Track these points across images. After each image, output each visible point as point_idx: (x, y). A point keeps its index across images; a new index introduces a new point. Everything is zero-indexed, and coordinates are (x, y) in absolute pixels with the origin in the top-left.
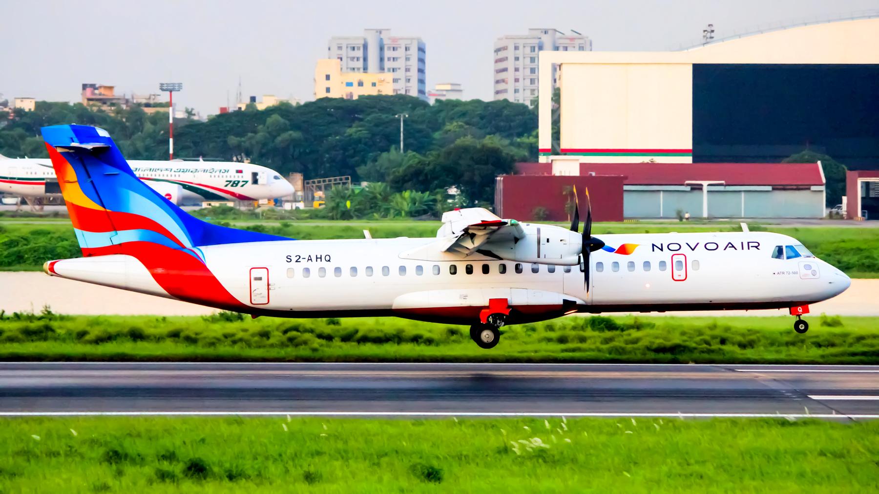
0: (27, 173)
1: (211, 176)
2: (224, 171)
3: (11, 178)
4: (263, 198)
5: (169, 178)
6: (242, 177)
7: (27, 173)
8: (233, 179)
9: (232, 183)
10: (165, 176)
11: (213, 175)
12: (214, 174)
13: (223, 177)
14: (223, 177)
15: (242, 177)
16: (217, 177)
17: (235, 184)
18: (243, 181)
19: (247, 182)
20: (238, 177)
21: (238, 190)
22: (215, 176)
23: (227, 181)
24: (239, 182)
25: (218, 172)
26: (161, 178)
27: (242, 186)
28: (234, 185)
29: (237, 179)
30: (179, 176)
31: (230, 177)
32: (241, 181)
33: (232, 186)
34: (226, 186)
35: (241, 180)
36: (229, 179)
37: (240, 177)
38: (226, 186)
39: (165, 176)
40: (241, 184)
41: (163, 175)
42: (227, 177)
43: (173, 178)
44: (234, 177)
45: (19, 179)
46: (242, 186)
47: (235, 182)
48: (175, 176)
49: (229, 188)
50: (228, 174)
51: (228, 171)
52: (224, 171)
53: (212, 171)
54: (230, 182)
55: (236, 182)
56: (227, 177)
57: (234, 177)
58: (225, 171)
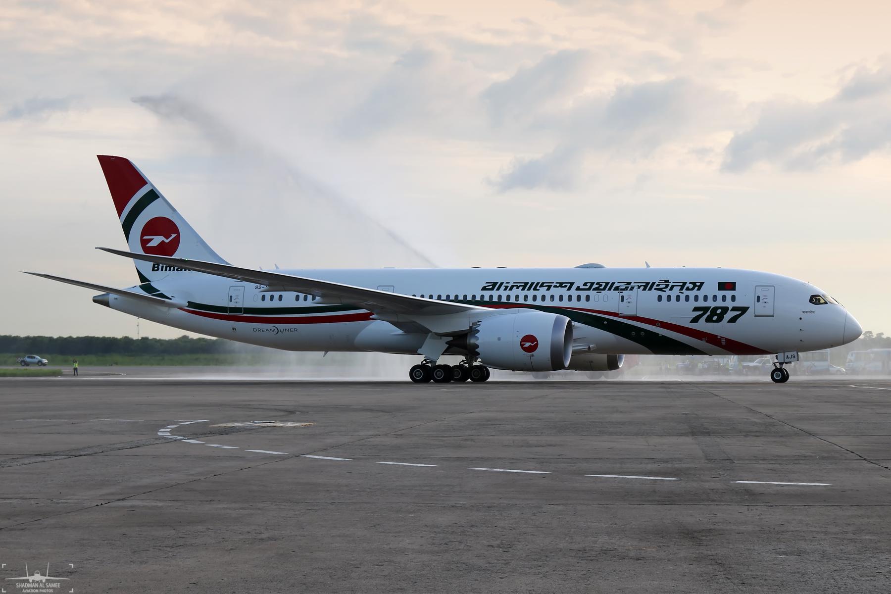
0: (263, 298)
1: (660, 298)
2: (691, 286)
5: (565, 304)
6: (733, 298)
8: (710, 304)
9: (708, 313)
10: (557, 298)
11: (664, 295)
12: (668, 292)
13: (687, 298)
14: (687, 298)
16: (673, 298)
17: (716, 315)
18: (734, 309)
19: (744, 310)
20: (724, 298)
22: (669, 298)
23: (696, 309)
24: (725, 310)
25: (676, 290)
26: (548, 303)
27: (733, 320)
28: (715, 318)
29: (719, 303)
31: (706, 298)
32: (730, 309)
33: (709, 320)
35: (729, 304)
36: (701, 303)
37: (729, 298)
38: (695, 320)
39: (557, 298)
40: (730, 315)
41: (552, 297)
42: (696, 298)
43: (574, 304)
44: (715, 298)
46: (733, 320)
47: (716, 308)
49: (702, 326)
50: (701, 294)
51: (702, 284)
52: (691, 286)
53: (661, 286)
54: (705, 309)
55: (719, 311)
56: (696, 298)
57: (715, 298)
58: (694, 284)
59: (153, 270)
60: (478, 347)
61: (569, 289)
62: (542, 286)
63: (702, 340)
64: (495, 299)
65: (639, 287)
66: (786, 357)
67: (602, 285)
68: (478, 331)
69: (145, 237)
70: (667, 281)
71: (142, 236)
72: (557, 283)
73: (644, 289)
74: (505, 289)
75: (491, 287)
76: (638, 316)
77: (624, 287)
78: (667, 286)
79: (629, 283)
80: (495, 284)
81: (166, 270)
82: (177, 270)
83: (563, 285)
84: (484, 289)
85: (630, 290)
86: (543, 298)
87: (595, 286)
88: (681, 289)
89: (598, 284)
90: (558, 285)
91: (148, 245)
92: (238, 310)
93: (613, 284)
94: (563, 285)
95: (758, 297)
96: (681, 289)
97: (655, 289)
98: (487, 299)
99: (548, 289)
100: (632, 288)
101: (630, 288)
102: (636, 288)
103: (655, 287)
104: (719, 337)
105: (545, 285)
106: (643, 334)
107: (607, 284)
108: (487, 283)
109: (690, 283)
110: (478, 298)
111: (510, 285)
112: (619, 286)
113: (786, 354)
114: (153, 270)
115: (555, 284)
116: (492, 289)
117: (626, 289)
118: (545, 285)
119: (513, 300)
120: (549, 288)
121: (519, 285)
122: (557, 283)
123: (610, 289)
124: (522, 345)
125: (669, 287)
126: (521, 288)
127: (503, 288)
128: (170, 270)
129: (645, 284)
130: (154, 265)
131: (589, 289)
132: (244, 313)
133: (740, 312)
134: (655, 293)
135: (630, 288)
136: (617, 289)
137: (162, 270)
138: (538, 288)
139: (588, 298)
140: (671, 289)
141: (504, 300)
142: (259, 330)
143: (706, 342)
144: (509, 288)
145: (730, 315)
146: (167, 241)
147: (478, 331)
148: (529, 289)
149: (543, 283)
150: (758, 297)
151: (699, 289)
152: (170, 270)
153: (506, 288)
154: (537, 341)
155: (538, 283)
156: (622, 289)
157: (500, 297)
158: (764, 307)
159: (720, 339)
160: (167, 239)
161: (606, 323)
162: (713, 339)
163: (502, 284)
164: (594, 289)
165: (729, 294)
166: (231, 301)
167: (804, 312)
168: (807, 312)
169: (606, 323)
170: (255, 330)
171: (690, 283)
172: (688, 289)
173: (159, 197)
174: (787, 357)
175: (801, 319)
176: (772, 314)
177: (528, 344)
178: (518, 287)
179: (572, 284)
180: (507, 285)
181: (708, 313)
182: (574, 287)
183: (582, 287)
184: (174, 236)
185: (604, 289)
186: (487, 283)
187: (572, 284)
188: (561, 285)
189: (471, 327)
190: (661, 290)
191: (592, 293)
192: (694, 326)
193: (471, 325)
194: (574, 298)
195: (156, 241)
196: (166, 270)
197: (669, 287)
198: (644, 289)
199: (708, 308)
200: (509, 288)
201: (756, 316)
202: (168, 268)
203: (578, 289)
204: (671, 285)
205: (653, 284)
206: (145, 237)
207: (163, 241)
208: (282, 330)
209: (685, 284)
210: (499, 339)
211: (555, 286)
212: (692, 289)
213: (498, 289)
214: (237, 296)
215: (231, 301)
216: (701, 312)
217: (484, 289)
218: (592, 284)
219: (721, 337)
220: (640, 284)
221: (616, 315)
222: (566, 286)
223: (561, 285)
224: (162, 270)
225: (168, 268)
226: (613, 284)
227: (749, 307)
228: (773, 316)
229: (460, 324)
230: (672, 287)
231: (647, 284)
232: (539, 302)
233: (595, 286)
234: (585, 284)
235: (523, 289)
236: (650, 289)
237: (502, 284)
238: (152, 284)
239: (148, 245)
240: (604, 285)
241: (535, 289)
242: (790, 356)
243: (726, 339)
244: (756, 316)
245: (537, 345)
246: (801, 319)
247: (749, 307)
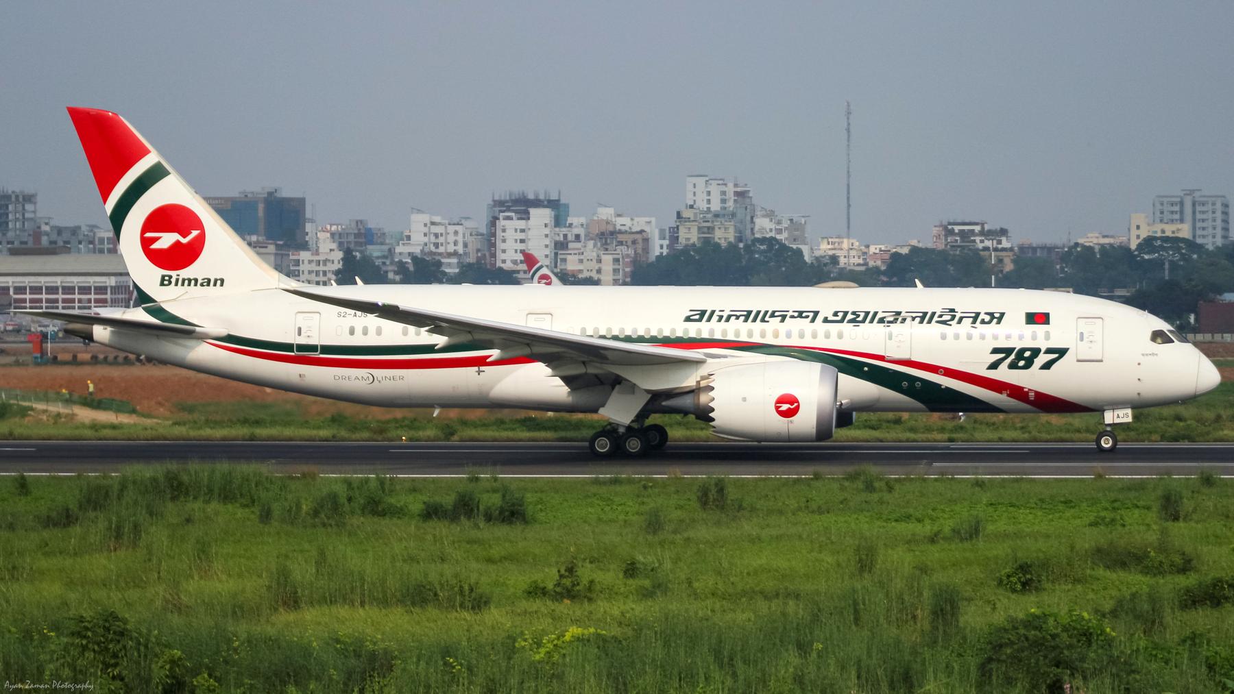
0: (352, 332)
1: (944, 337)
3: (301, 348)
4: (1116, 404)
6: (1047, 336)
7: (352, 332)
9: (1013, 357)
15: (1047, 336)
17: (1024, 358)
18: (1049, 351)
19: (1062, 352)
21: (1032, 379)
22: (957, 337)
23: (996, 351)
24: (1036, 352)
27: (1047, 366)
28: (1022, 363)
30: (840, 336)
32: (1043, 351)
33: (1013, 366)
34: (994, 366)
38: (994, 366)
40: (1043, 359)
45: (327, 349)
46: (1047, 366)
47: (1023, 350)
48: (827, 336)
49: (1004, 374)
51: (1002, 314)
52: (987, 318)
54: (1008, 351)
55: (1027, 354)
58: (992, 315)
59: (162, 284)
60: (713, 410)
61: (813, 321)
62: (773, 315)
63: (1001, 393)
64: (705, 335)
65: (914, 319)
66: (1116, 416)
67: (859, 316)
68: (712, 389)
69: (148, 235)
70: (952, 310)
71: (144, 230)
72: (794, 312)
73: (921, 322)
74: (720, 320)
75: (697, 317)
76: (914, 359)
77: (891, 319)
78: (953, 317)
79: (899, 313)
80: (703, 313)
81: (183, 285)
82: (202, 285)
83: (804, 315)
84: (688, 319)
85: (902, 322)
86: (776, 335)
87: (850, 317)
88: (974, 322)
89: (854, 313)
90: (796, 314)
91: (155, 246)
92: (313, 348)
93: (876, 313)
94: (804, 315)
95: (1082, 334)
96: (974, 322)
97: (937, 322)
98: (692, 334)
99: (782, 321)
100: (904, 320)
101: (900, 319)
102: (909, 320)
103: (936, 318)
104: (1025, 390)
105: (776, 314)
106: (918, 384)
107: (867, 313)
108: (691, 310)
109: (986, 313)
110: (679, 334)
111: (725, 315)
112: (885, 317)
113: (1117, 412)
114: (162, 284)
115: (789, 314)
116: (700, 320)
117: (895, 321)
118: (776, 314)
119: (731, 337)
120: (784, 318)
121: (738, 314)
122: (794, 312)
123: (872, 321)
124: (777, 408)
125: (957, 319)
126: (742, 318)
127: (715, 318)
128: (189, 285)
129: (921, 314)
130: (163, 277)
131: (842, 321)
132: (321, 353)
133: (1056, 355)
134: (935, 329)
135: (900, 319)
136: (881, 321)
137: (176, 284)
138: (767, 319)
139: (840, 336)
140: (960, 322)
141: (718, 336)
142: (343, 378)
143: (1008, 395)
144: (724, 319)
145: (1043, 359)
146: (184, 241)
147: (712, 389)
148: (754, 320)
149: (774, 312)
150: (1082, 334)
151: (999, 322)
152: (189, 285)
153: (721, 317)
154: (798, 402)
155: (766, 312)
156: (889, 322)
157: (712, 331)
158: (1090, 348)
159: (1027, 393)
160: (184, 237)
161: (866, 369)
162: (1017, 392)
163: (713, 312)
164: (850, 321)
165: (1040, 329)
166: (300, 334)
167: (1143, 355)
168: (1147, 355)
169: (866, 369)
170: (337, 378)
171: (986, 313)
172: (983, 322)
173: (169, 173)
174: (1118, 417)
175: (1139, 364)
176: (1100, 358)
177: (785, 407)
178: (738, 317)
179: (816, 313)
180: (721, 313)
181: (1013, 357)
182: (820, 318)
183: (831, 318)
184: (195, 233)
185: (863, 321)
186: (691, 310)
187: (816, 313)
188: (800, 314)
189: (698, 382)
190: (944, 322)
191: (846, 327)
192: (992, 374)
193: (699, 379)
194: (821, 335)
195: (166, 240)
196: (183, 285)
197: (957, 319)
198: (921, 322)
199: (1011, 350)
200: (724, 319)
201: (1078, 361)
202: (186, 282)
203: (826, 320)
204: (958, 316)
205: (934, 314)
206: (148, 235)
207: (178, 242)
208: (380, 379)
209: (978, 314)
210: (744, 399)
211: (792, 317)
212: (990, 322)
213: (709, 320)
214: (310, 327)
215: (300, 334)
216: (1002, 356)
217: (688, 319)
218: (846, 313)
219: (1030, 390)
220: (914, 315)
221: (881, 358)
222: (807, 317)
223: (800, 314)
224: (176, 284)
225: (186, 282)
226: (876, 313)
227: (1068, 349)
228: (1102, 361)
229: (689, 380)
230: (961, 319)
231: (926, 314)
232: (769, 340)
233: (850, 317)
234: (836, 314)
235: (746, 321)
236: (929, 322)
237: (713, 312)
238: (164, 306)
239: (155, 246)
240: (862, 315)
241: (763, 320)
242: (1121, 415)
243: (1038, 394)
244: (1078, 361)
245: (798, 407)
246: (1139, 364)
247: (1068, 349)
